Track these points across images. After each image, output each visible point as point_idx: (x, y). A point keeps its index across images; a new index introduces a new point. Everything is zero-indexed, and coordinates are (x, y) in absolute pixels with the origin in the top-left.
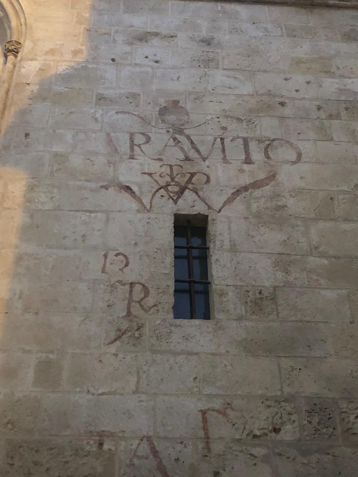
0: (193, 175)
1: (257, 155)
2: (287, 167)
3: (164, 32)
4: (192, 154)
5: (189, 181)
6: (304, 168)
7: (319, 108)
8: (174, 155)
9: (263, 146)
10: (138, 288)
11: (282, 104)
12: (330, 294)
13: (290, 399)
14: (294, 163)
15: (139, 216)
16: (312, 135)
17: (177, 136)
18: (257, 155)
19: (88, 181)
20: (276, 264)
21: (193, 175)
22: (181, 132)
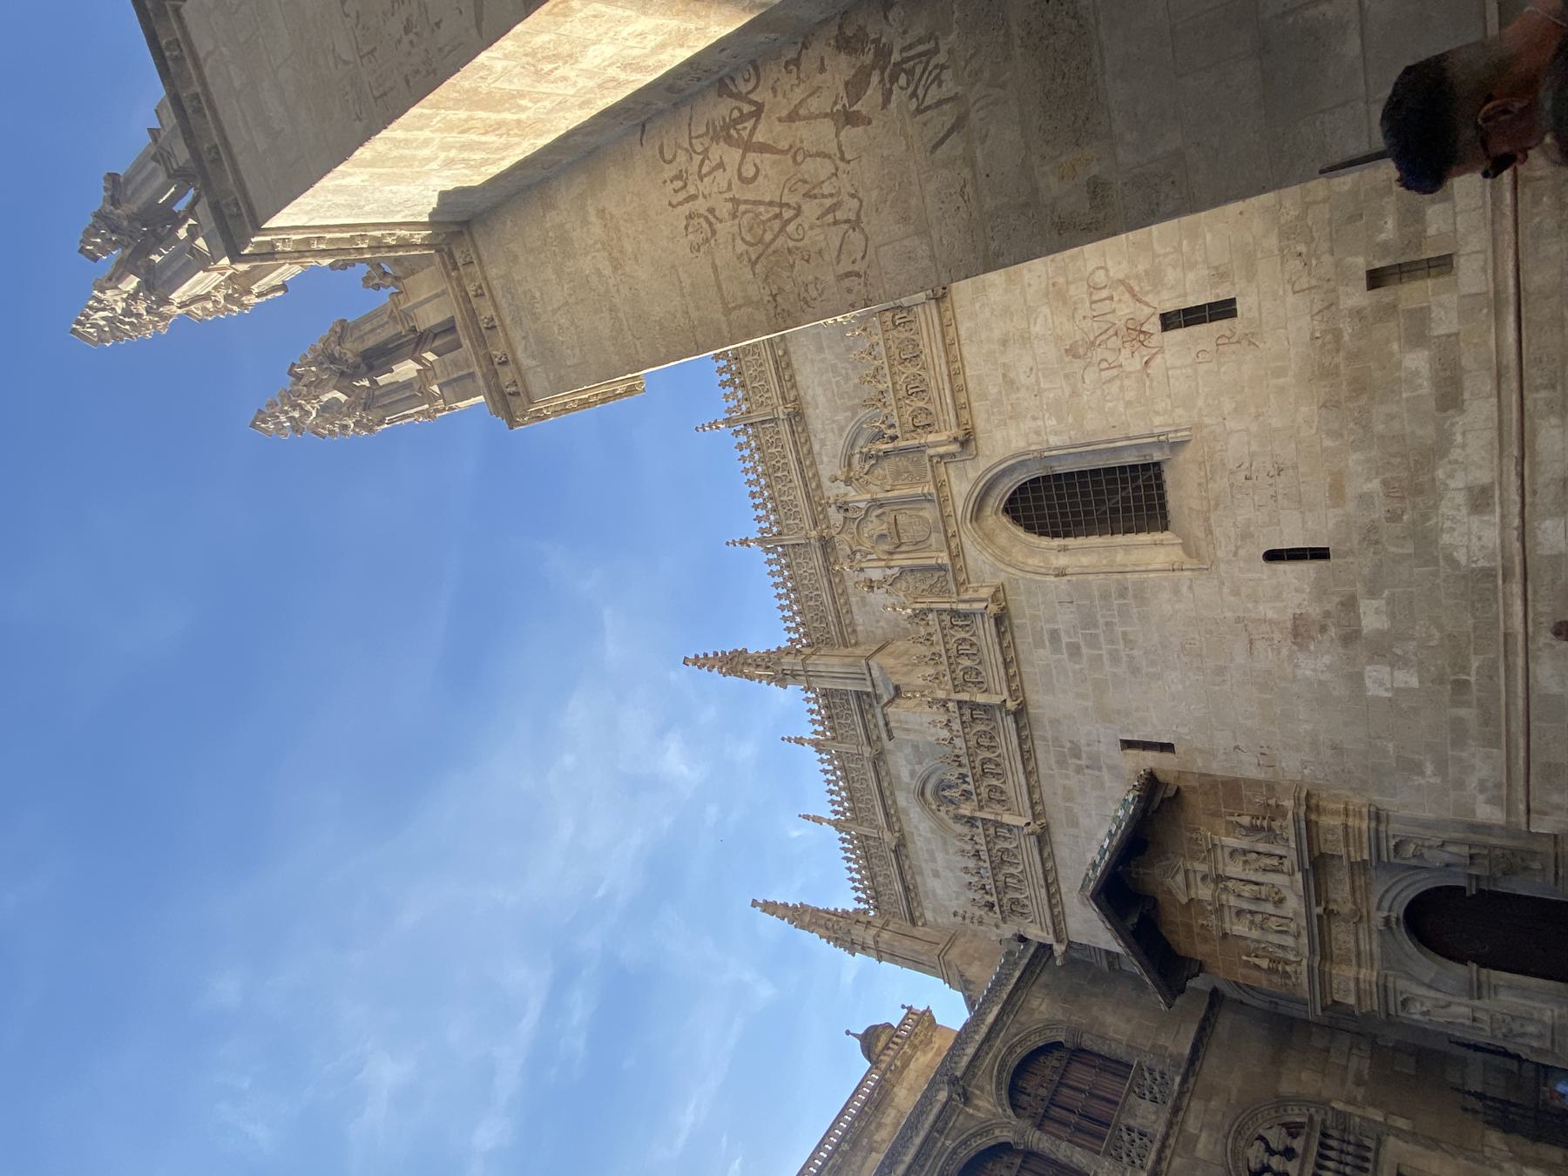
1: (1104, 293)
3: (1001, 371)
4: (1111, 332)
6: (1110, 264)
8: (1114, 342)
12: (1209, 237)
13: (1281, 250)
18: (1104, 293)
22: (1093, 343)
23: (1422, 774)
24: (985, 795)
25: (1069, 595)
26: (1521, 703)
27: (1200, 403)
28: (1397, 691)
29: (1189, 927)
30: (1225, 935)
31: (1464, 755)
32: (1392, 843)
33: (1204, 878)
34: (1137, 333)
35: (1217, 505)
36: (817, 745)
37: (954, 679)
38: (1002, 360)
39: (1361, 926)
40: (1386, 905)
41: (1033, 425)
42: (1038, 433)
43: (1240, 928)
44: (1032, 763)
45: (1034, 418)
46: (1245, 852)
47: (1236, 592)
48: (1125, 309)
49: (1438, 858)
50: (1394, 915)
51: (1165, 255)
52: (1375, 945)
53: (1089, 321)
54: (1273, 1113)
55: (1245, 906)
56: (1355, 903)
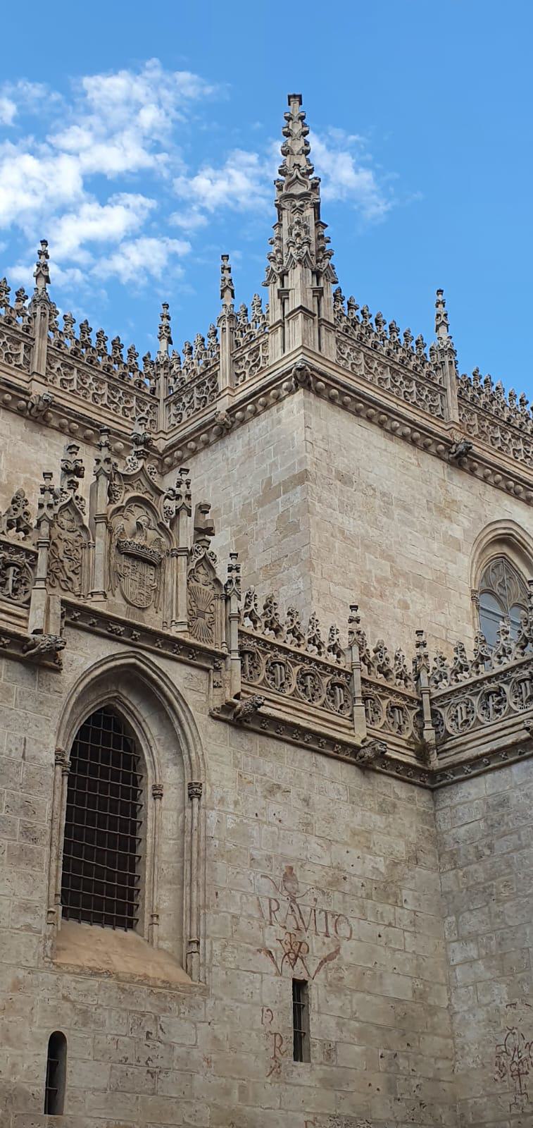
0: (301, 943)
1: (331, 930)
2: (345, 942)
5: (299, 951)
6: (353, 943)
7: (363, 886)
8: (291, 924)
9: (334, 920)
10: (278, 1037)
11: (345, 878)
12: (357, 1049)
14: (349, 939)
15: (276, 978)
16: (357, 914)
17: (292, 904)
18: (331, 930)
19: (251, 944)
20: (338, 1024)
21: (301, 943)
22: (294, 901)
25: (34, 758)
27: (227, 1001)
34: (296, 953)
35: (123, 990)
38: (293, 794)
41: (231, 798)
42: (222, 800)
45: (236, 803)
47: (17, 986)
48: (317, 946)
51: (351, 1002)
53: (312, 903)
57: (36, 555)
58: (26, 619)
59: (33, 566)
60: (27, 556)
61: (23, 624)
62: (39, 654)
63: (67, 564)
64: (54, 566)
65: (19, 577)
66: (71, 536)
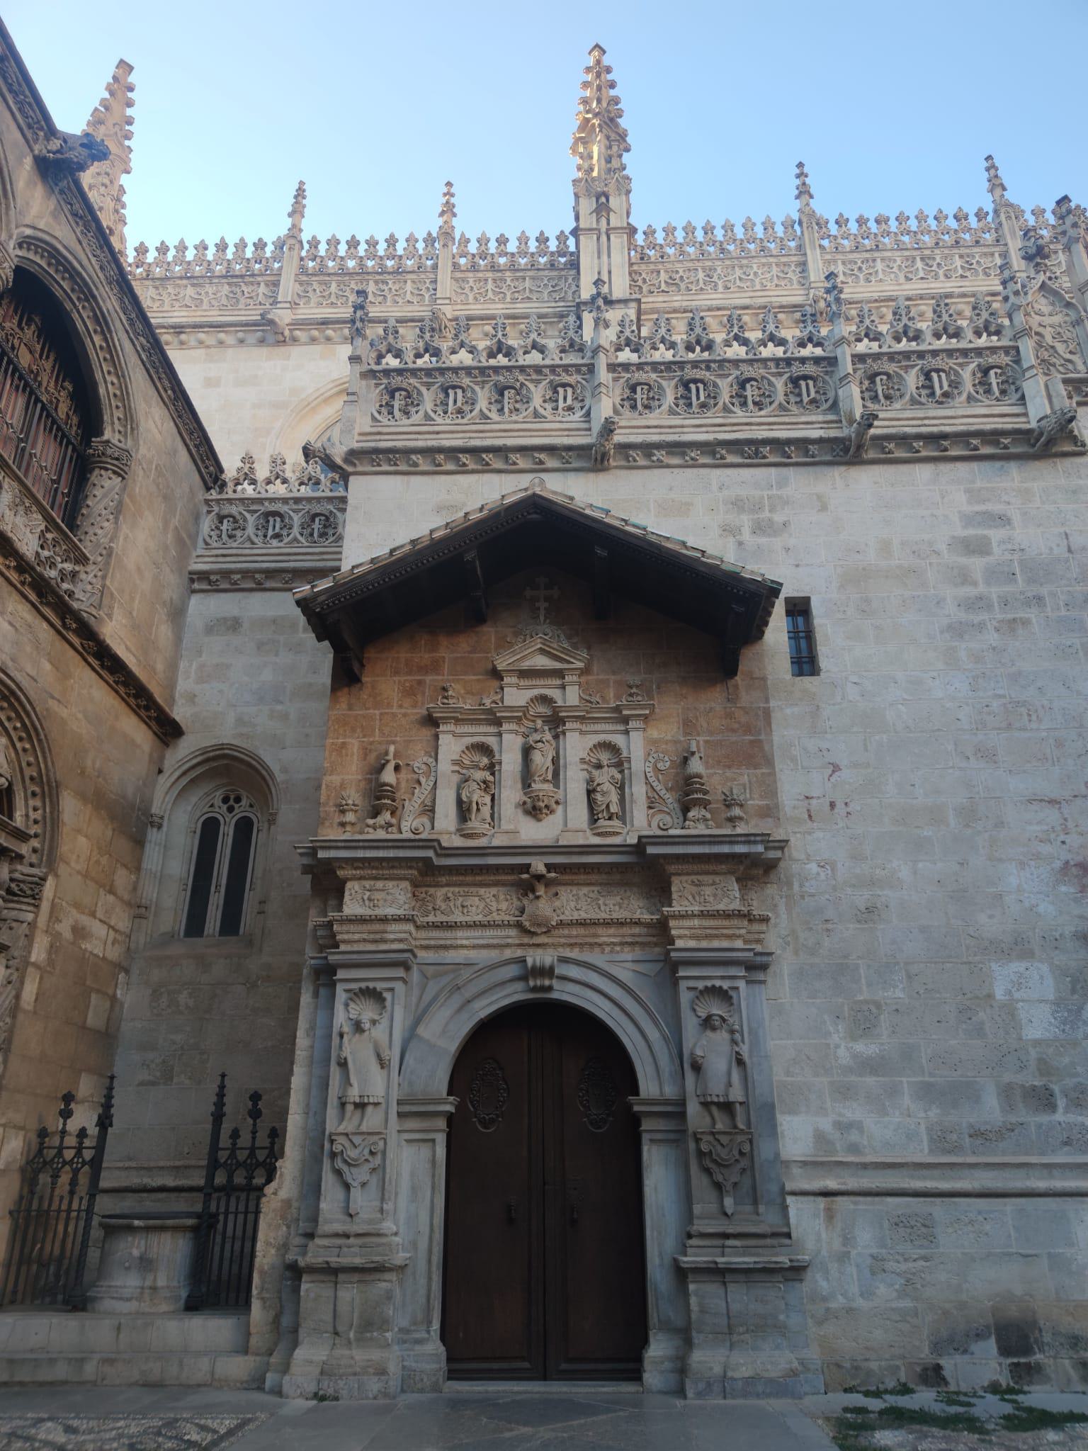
23: (853, 1038)
24: (640, 376)
26: (1041, 1185)
28: (1009, 1010)
29: (435, 667)
30: (431, 721)
31: (906, 1101)
32: (725, 985)
33: (545, 700)
36: (447, 234)
37: (876, 357)
39: (513, 932)
40: (573, 972)
43: (451, 745)
44: (731, 459)
46: (619, 765)
49: (713, 1051)
50: (555, 983)
52: (472, 954)
54: (30, 772)
55: (510, 761)
56: (561, 924)
57: (1017, 349)
58: (1026, 415)
59: (1018, 361)
60: (1007, 353)
61: (1023, 419)
62: (1051, 442)
63: (1060, 348)
64: (1046, 355)
65: (1004, 378)
66: (1057, 319)
